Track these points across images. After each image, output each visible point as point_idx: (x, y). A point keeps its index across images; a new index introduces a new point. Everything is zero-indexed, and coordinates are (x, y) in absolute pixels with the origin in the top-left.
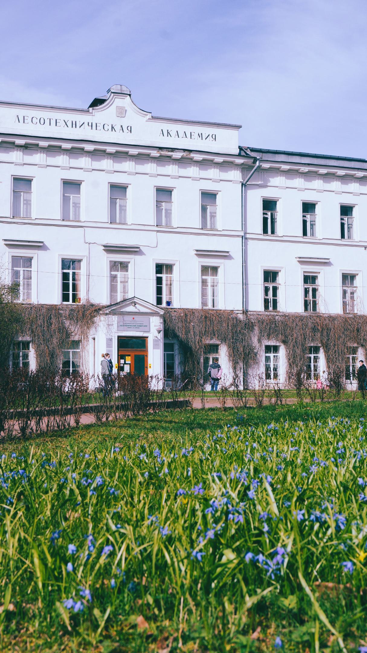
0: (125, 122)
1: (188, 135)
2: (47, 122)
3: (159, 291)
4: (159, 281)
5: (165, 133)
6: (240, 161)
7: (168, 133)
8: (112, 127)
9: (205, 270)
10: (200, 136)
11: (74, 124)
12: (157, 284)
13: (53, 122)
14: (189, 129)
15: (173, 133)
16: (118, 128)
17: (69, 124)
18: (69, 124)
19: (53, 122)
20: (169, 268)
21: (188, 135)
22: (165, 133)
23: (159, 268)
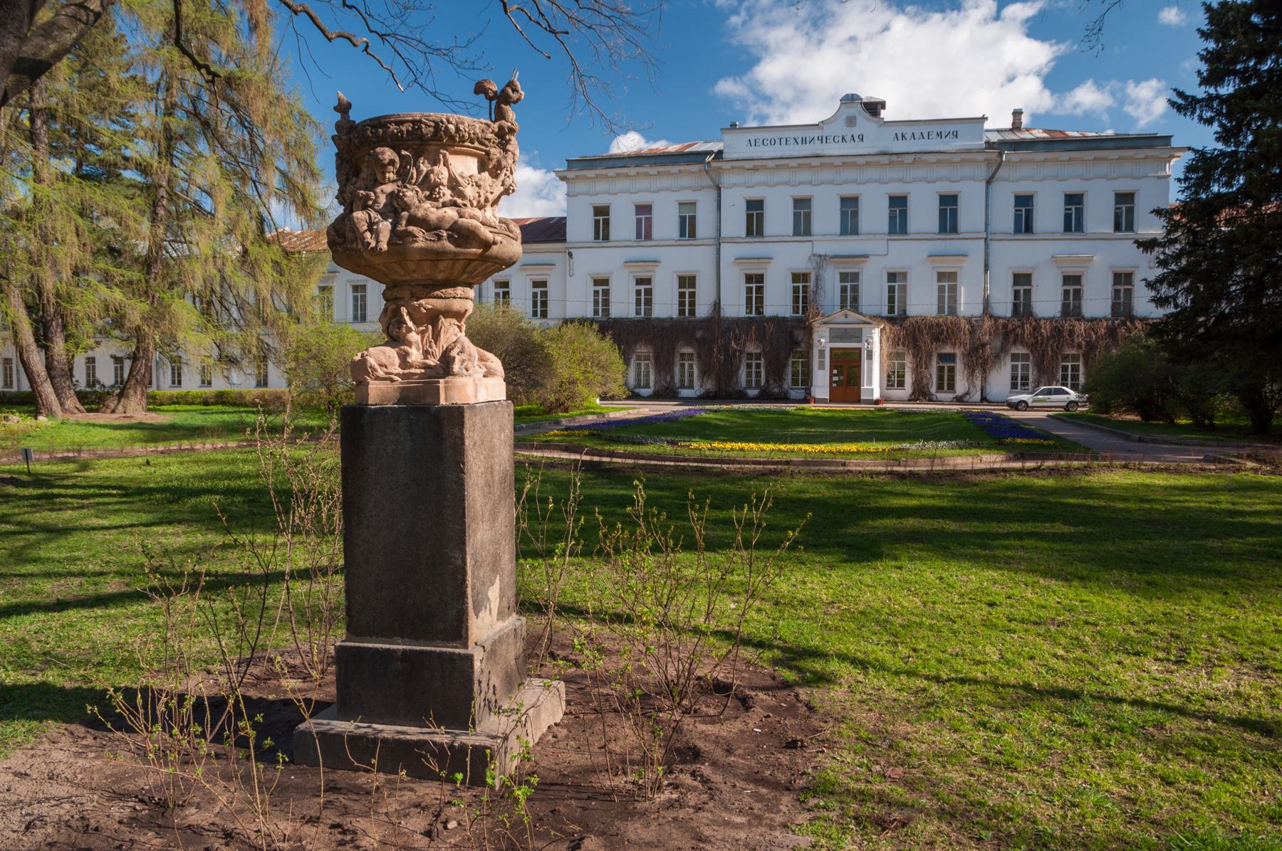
0: (856, 131)
1: (926, 135)
2: (778, 142)
3: (891, 299)
4: (891, 289)
5: (900, 137)
6: (981, 157)
7: (903, 136)
8: (843, 138)
9: (941, 276)
10: (939, 134)
11: (804, 141)
12: (762, 298)
13: (783, 141)
14: (925, 130)
15: (908, 136)
16: (848, 138)
17: (799, 141)
18: (799, 141)
19: (783, 141)
20: (904, 275)
21: (926, 135)
22: (900, 137)
23: (892, 277)
